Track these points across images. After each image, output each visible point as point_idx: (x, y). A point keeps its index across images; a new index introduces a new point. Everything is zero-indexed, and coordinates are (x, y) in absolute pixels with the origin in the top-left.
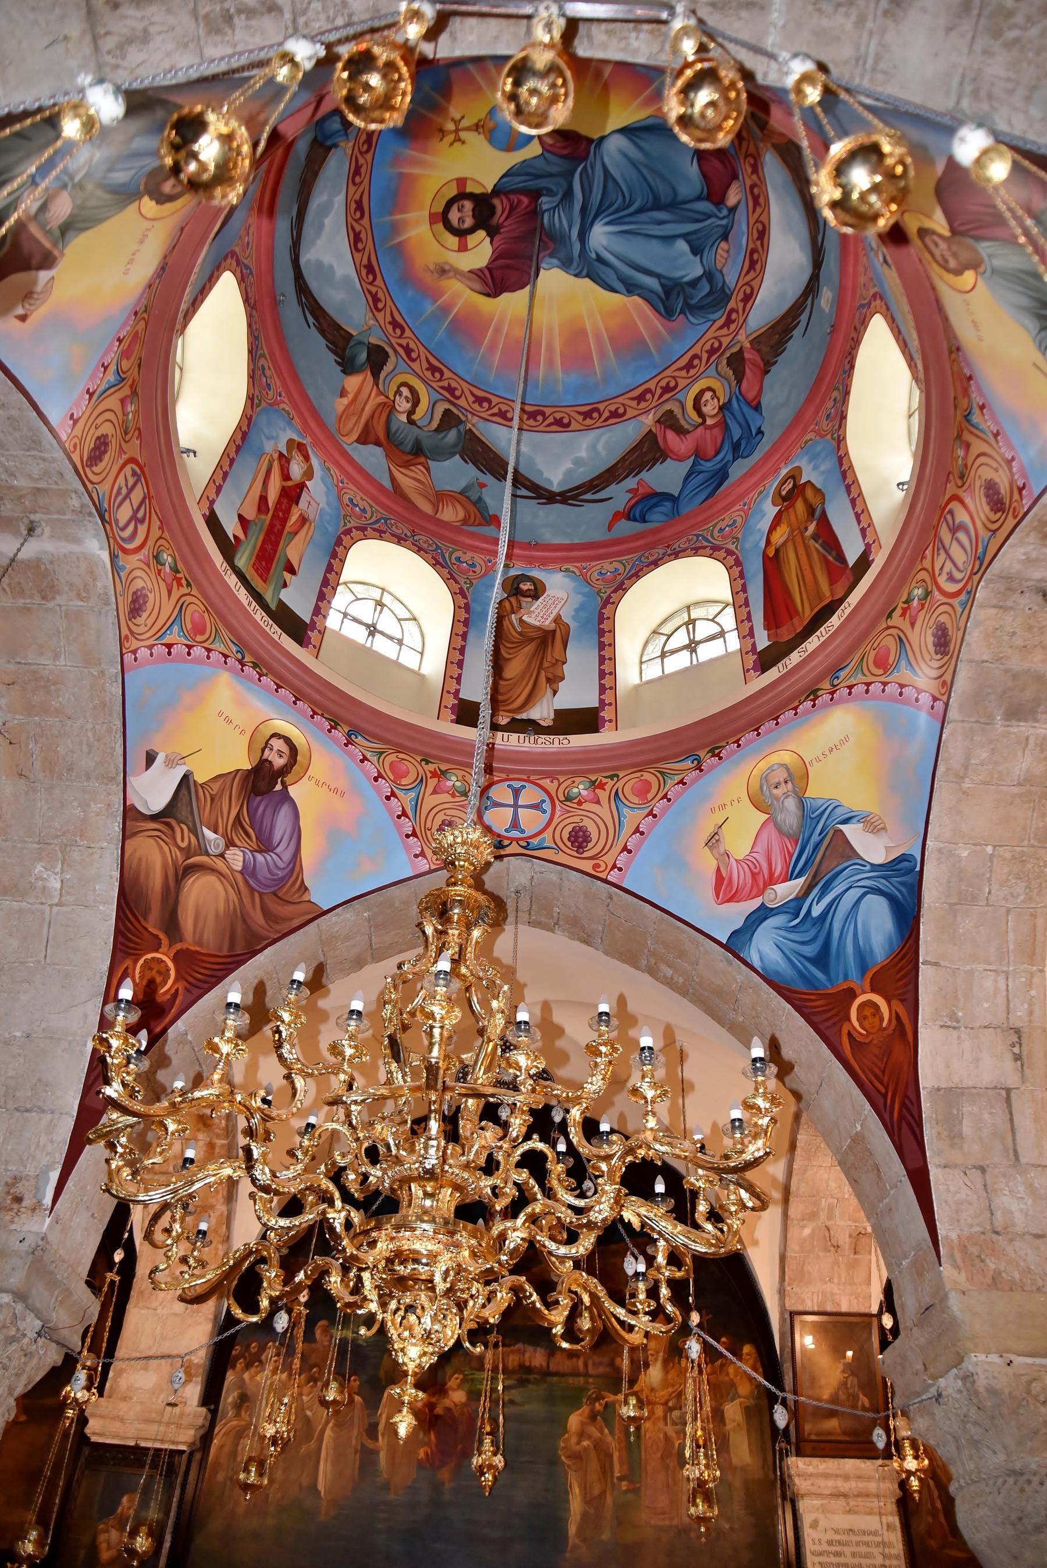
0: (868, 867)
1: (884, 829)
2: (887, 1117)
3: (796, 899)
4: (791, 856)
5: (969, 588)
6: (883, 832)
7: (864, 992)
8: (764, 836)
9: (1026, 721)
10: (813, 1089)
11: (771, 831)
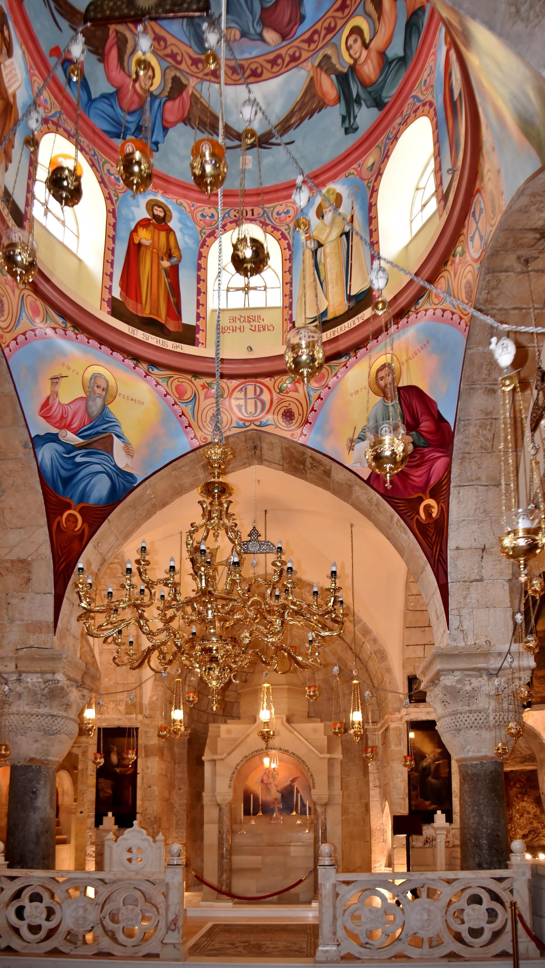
0: (113, 464)
1: (132, 456)
2: (57, 566)
3: (73, 446)
4: (84, 426)
7: (75, 510)
8: (79, 403)
11: (81, 405)
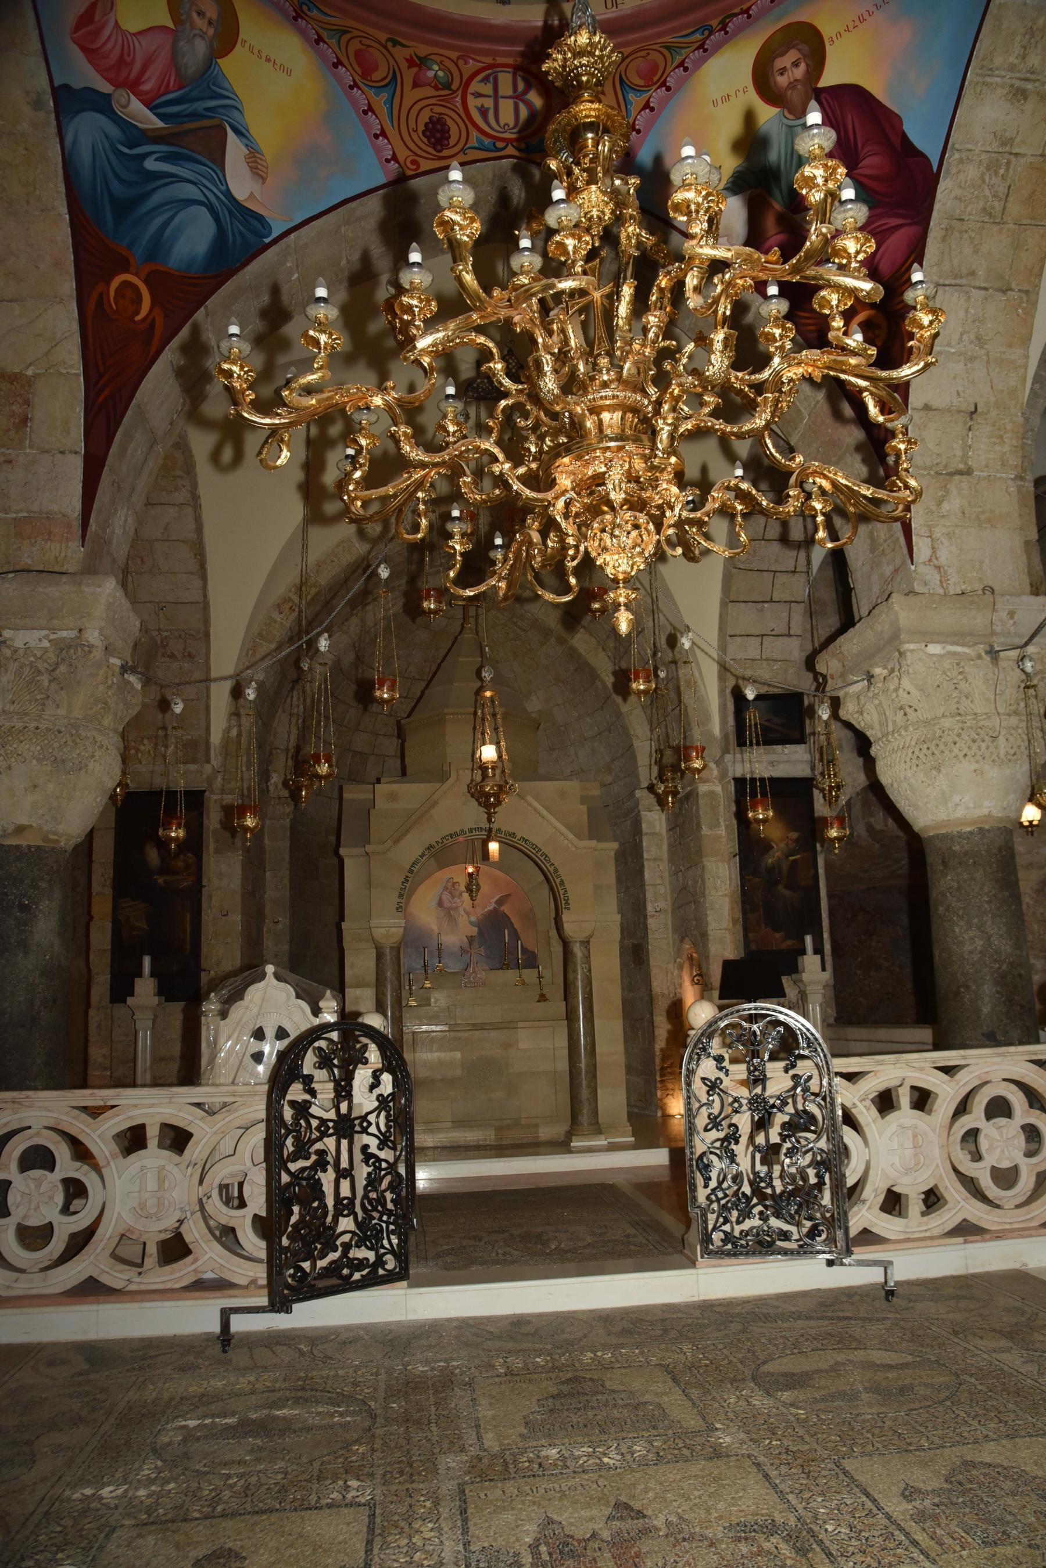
3: (143, 131)
4: (166, 93)
5: (500, 145)
6: (261, 181)
7: (136, 275)
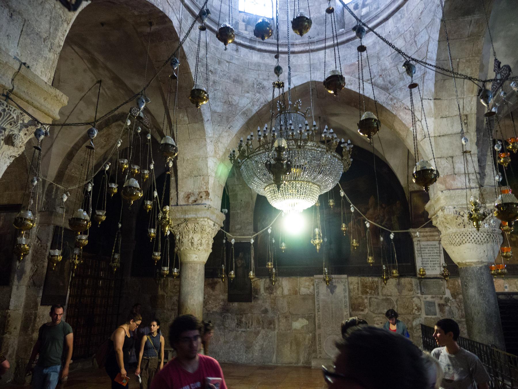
9: (470, 15)
10: (405, 137)
